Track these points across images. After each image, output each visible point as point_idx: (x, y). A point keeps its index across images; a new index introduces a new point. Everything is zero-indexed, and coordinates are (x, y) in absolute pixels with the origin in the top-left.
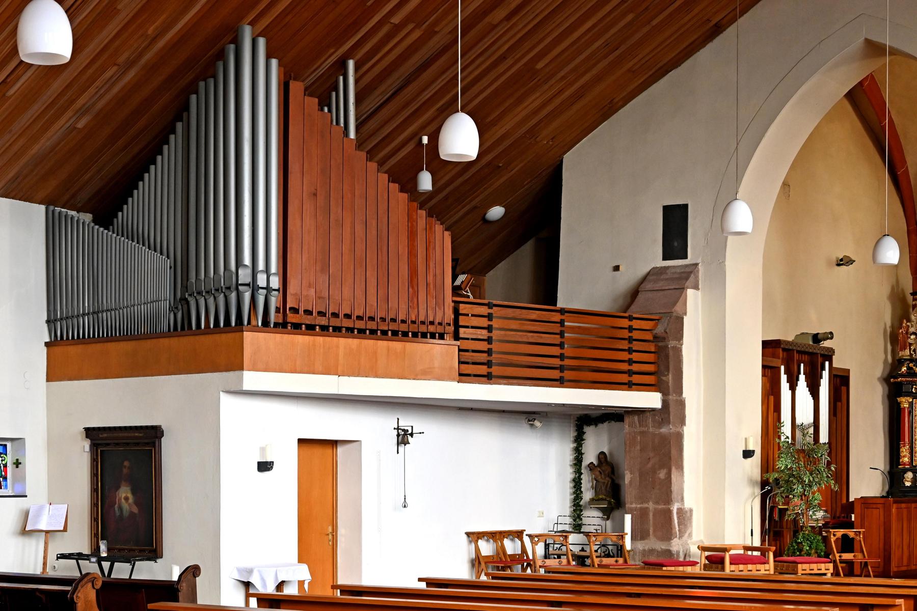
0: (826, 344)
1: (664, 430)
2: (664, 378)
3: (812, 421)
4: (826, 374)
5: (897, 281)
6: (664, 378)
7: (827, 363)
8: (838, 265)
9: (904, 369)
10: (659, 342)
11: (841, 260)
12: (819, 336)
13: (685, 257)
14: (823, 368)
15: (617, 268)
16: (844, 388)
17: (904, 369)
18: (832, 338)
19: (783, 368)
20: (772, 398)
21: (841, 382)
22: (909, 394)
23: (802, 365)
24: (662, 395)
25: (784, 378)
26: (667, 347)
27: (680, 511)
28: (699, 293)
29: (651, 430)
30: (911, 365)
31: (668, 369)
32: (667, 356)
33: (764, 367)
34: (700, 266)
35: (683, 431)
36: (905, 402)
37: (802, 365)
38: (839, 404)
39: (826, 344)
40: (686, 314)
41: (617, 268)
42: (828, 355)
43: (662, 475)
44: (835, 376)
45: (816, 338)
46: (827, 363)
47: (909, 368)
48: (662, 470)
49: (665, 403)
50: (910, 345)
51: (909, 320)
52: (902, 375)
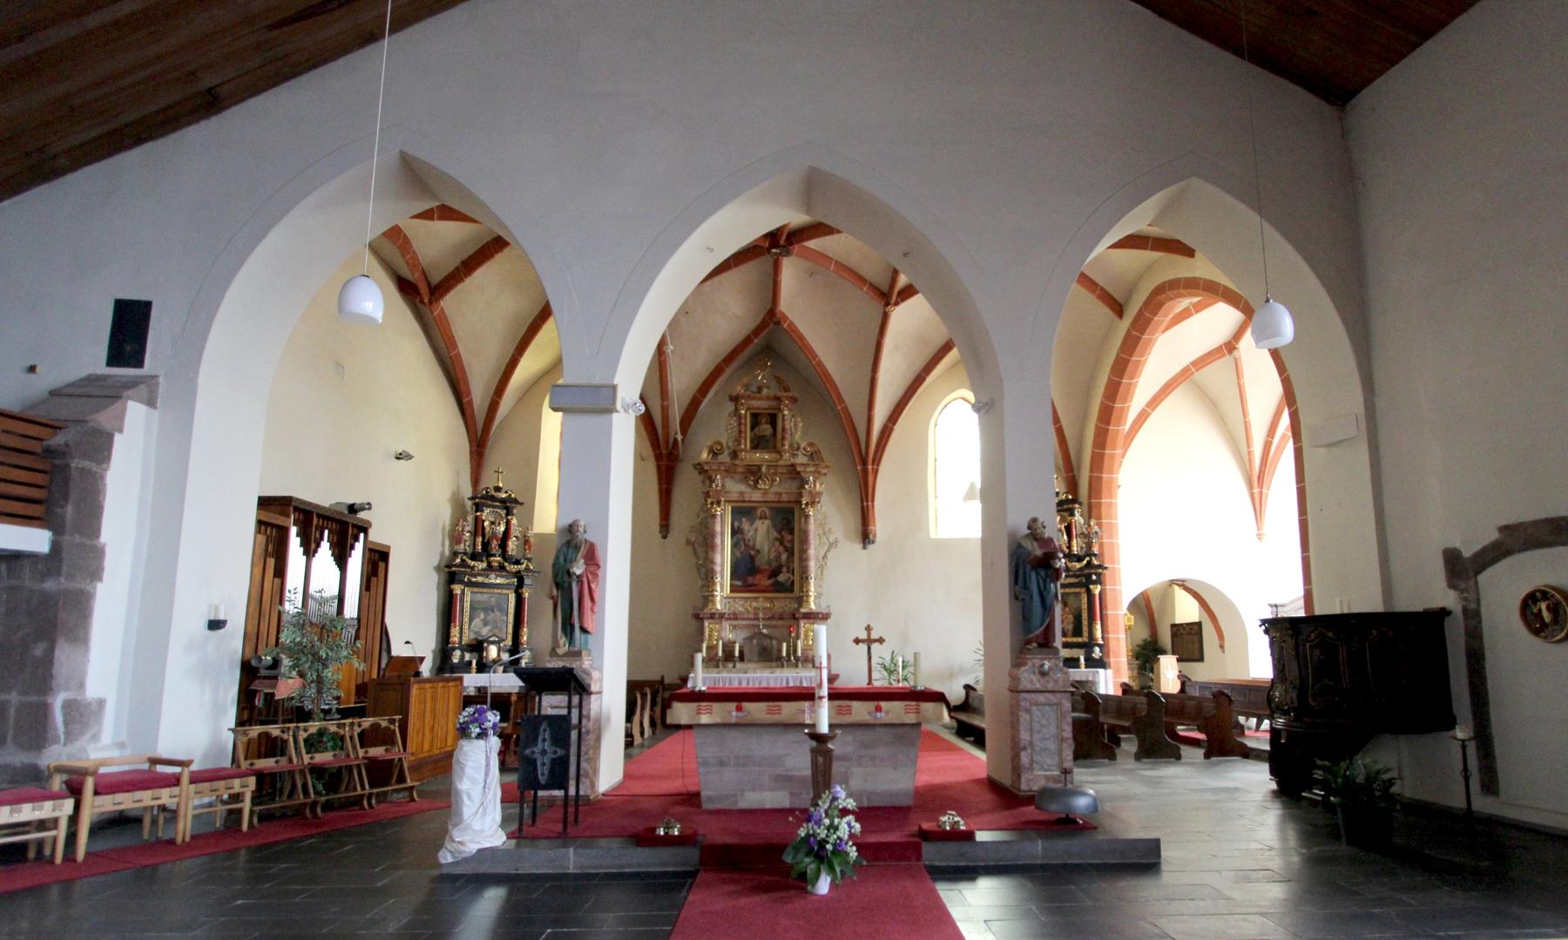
0: (362, 515)
1: (50, 585)
2: (59, 511)
3: (337, 593)
4: (359, 546)
5: (458, 488)
6: (59, 511)
7: (362, 535)
8: (398, 458)
9: (458, 560)
10: (54, 458)
11: (400, 454)
12: (355, 506)
13: (139, 363)
14: (357, 539)
15: (32, 369)
16: (381, 565)
17: (458, 560)
18: (370, 509)
19: (294, 530)
20: (271, 562)
21: (378, 560)
22: (461, 582)
23: (326, 532)
24: (53, 534)
25: (294, 542)
26: (67, 466)
27: (69, 706)
28: (156, 414)
29: (28, 583)
30: (464, 557)
31: (66, 497)
32: (66, 481)
33: (260, 523)
34: (161, 380)
35: (95, 589)
36: (457, 589)
37: (326, 532)
38: (374, 579)
39: (362, 515)
40: (121, 431)
41: (32, 369)
42: (364, 528)
43: (39, 650)
44: (371, 550)
45: (353, 509)
46: (362, 535)
47: (462, 560)
48: (39, 644)
49: (56, 547)
50: (465, 541)
51: (465, 520)
52: (456, 566)
